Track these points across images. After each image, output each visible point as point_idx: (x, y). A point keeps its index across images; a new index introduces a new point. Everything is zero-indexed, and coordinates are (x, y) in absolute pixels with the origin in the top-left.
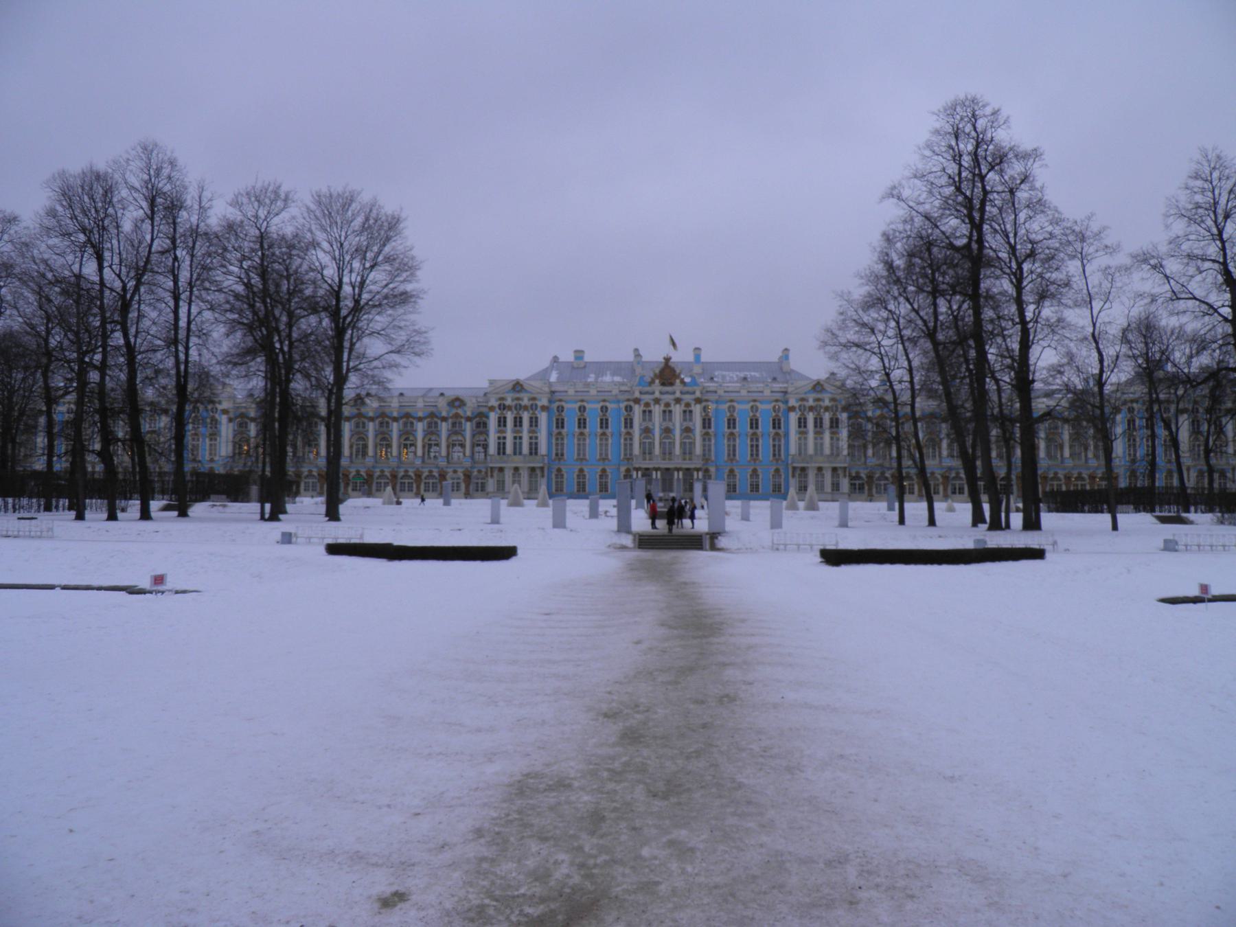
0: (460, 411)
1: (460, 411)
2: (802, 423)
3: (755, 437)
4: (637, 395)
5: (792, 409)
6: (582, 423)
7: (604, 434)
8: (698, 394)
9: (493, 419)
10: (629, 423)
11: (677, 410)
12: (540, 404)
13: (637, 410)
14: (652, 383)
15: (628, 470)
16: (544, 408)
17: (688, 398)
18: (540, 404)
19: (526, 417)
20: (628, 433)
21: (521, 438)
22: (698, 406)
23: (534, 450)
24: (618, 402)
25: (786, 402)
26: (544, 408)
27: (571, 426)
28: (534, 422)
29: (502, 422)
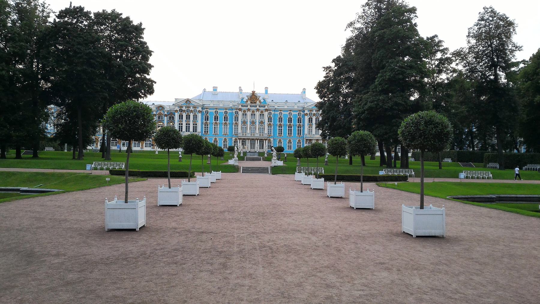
1: (162, 112)
3: (290, 127)
4: (240, 107)
5: (306, 114)
6: (216, 118)
7: (226, 123)
8: (266, 107)
10: (237, 119)
11: (257, 114)
13: (240, 113)
14: (247, 101)
15: (236, 139)
16: (199, 111)
18: (198, 110)
20: (236, 123)
21: (189, 124)
22: (266, 112)
24: (232, 109)
25: (304, 111)
27: (212, 120)
28: (195, 117)
29: (181, 117)
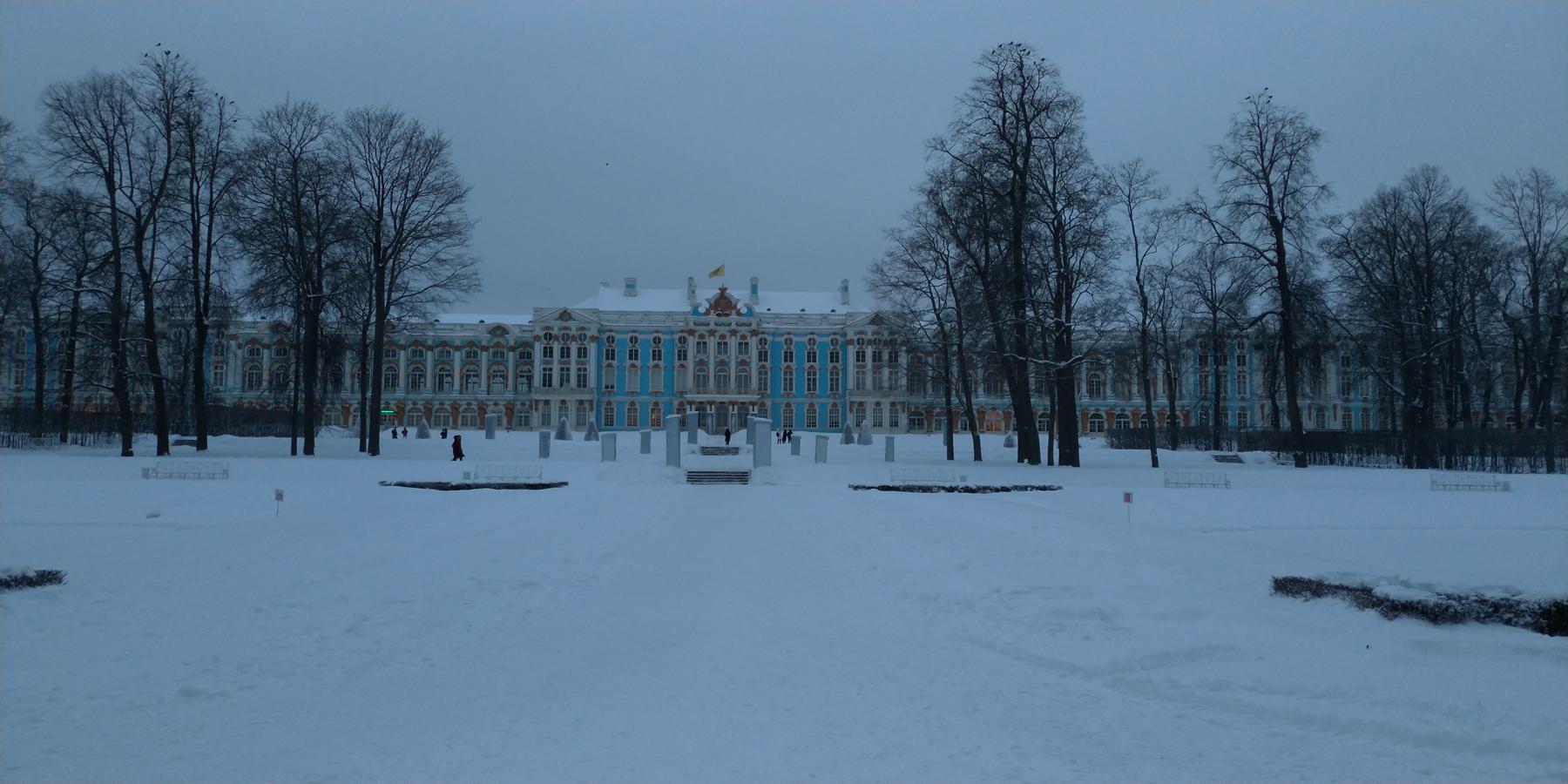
0: (501, 340)
1: (501, 340)
2: (860, 356)
4: (692, 326)
5: (851, 342)
8: (754, 326)
9: (538, 348)
10: (683, 355)
11: (733, 342)
12: (589, 334)
13: (692, 342)
15: (681, 404)
16: (593, 338)
17: (744, 330)
18: (589, 334)
19: (574, 347)
23: (582, 381)
25: (845, 335)
26: (593, 338)
28: (583, 352)
29: (548, 352)
